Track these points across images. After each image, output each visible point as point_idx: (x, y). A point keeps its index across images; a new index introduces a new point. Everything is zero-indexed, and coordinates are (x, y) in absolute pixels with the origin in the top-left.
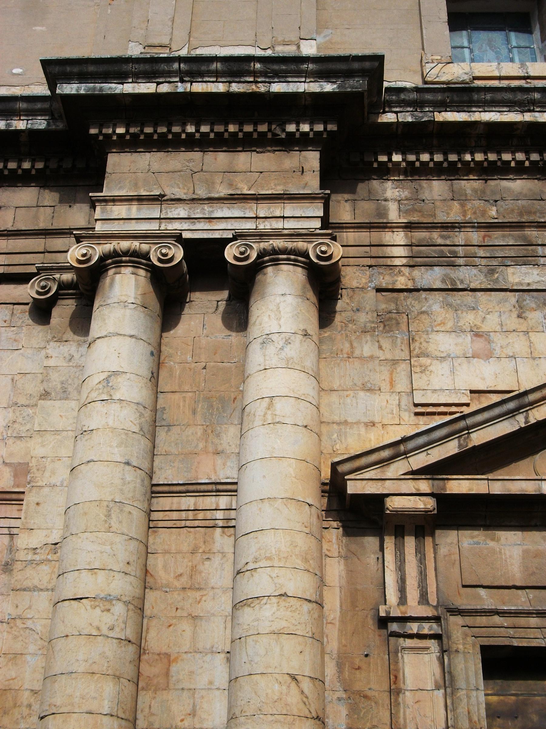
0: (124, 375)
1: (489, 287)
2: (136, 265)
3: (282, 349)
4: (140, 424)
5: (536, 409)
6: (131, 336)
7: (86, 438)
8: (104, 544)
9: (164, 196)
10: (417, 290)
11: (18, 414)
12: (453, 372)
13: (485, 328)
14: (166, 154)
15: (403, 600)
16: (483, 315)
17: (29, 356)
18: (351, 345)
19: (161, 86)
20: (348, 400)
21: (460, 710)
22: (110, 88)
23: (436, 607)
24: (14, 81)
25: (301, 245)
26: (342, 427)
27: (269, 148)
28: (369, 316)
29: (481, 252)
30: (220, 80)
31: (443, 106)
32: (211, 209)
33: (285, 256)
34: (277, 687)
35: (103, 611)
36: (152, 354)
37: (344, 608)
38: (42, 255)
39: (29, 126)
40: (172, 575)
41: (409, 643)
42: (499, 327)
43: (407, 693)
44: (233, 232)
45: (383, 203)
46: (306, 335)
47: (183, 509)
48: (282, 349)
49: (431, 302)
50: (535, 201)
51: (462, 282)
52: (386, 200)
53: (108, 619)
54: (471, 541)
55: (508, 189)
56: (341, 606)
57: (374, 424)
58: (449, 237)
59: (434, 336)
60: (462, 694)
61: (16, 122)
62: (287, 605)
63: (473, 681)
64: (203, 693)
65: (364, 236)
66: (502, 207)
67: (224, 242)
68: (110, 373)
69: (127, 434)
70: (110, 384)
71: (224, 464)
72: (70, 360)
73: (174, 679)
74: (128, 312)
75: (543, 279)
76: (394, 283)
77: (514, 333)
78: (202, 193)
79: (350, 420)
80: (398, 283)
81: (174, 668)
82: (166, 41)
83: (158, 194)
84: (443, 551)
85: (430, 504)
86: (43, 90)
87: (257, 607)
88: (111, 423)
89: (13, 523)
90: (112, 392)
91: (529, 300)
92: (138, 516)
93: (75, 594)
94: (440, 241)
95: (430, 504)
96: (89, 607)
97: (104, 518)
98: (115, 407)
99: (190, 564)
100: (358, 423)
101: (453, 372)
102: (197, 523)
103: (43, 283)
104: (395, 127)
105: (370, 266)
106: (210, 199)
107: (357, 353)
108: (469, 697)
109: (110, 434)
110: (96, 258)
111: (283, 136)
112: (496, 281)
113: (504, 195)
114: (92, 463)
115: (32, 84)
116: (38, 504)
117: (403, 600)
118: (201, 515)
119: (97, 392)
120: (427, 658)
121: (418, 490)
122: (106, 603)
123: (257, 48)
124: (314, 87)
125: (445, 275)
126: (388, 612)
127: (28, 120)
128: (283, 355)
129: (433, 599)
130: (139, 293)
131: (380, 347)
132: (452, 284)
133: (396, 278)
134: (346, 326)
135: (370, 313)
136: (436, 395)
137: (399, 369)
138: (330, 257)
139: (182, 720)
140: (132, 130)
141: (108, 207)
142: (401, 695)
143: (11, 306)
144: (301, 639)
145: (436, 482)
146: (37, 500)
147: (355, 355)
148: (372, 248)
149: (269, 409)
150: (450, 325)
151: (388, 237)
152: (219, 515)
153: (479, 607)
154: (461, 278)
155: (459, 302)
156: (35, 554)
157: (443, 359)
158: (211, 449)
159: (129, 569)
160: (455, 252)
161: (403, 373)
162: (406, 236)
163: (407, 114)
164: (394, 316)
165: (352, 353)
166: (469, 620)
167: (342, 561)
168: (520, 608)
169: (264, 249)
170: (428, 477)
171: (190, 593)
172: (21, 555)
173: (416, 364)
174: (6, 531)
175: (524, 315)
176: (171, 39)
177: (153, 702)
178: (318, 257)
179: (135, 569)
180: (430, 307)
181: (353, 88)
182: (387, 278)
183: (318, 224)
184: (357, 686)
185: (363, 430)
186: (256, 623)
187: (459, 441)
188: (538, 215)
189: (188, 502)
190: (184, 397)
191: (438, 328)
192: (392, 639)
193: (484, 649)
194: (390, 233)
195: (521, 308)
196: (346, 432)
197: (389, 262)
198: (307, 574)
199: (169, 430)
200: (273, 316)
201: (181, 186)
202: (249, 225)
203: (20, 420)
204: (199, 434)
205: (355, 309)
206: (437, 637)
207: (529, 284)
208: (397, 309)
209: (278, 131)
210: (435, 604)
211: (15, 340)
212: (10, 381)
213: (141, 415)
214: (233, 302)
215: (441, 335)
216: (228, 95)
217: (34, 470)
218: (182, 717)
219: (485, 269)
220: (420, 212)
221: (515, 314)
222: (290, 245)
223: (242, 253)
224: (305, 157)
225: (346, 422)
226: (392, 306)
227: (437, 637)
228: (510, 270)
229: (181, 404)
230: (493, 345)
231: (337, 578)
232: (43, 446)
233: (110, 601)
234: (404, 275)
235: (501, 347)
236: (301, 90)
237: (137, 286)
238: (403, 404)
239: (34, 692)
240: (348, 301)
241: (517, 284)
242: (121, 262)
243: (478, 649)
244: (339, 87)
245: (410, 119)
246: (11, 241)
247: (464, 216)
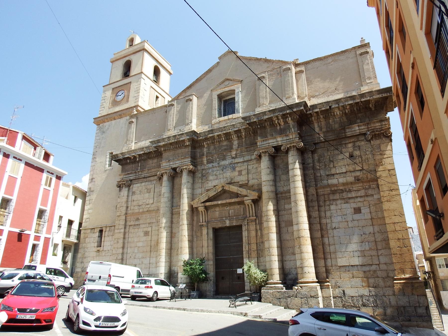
36: (170, 188)
55: (223, 145)
60: (209, 235)
74: (166, 182)
94: (211, 158)
213: (168, 198)
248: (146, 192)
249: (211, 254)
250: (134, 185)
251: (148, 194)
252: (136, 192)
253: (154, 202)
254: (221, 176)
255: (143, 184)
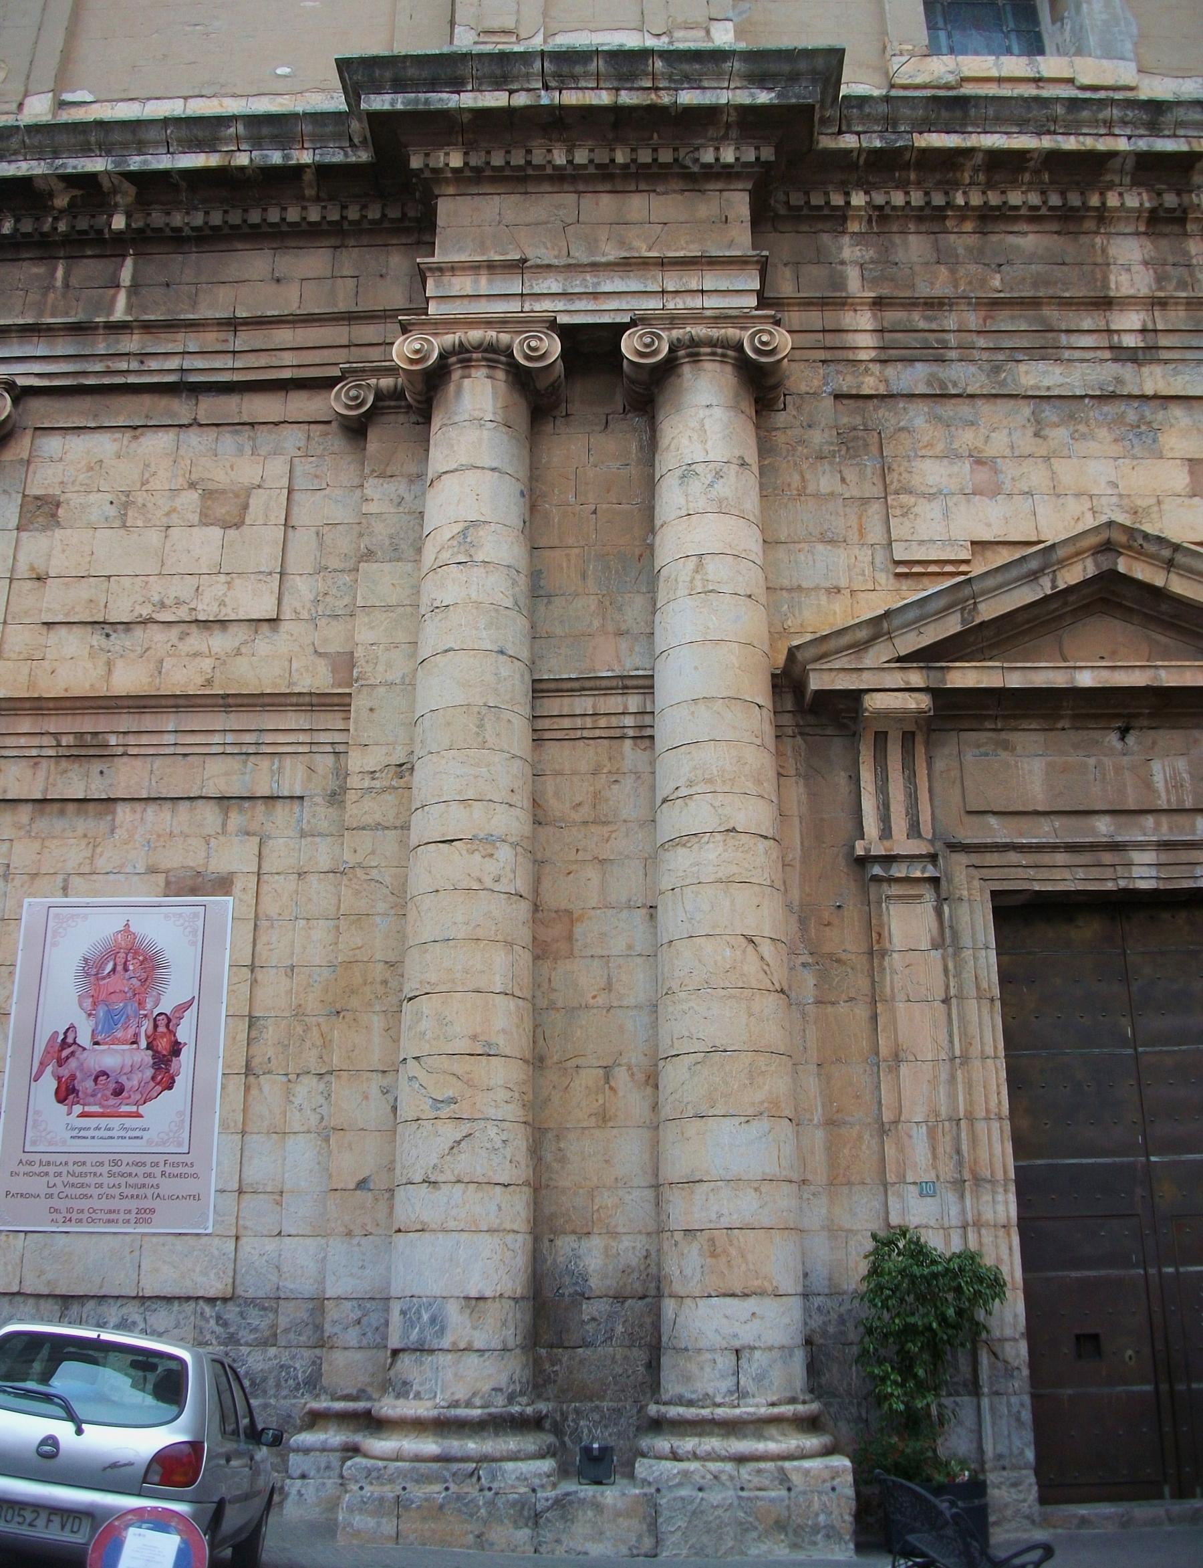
0: (487, 527)
1: (994, 392)
2: (492, 365)
3: (710, 485)
4: (513, 596)
5: (1066, 569)
6: (493, 470)
7: (440, 617)
8: (478, 765)
9: (525, 261)
10: (892, 396)
11: (330, 582)
12: (946, 515)
13: (990, 452)
14: (523, 197)
15: (886, 832)
16: (987, 433)
17: (339, 498)
18: (803, 477)
19: (515, 96)
20: (802, 557)
21: (965, 975)
22: (441, 100)
23: (932, 842)
24: (279, 86)
25: (732, 333)
26: (795, 595)
27: (677, 188)
28: (826, 435)
29: (982, 342)
30: (602, 85)
31: (927, 126)
32: (595, 280)
33: (708, 350)
34: (728, 952)
35: (484, 857)
36: (522, 494)
37: (806, 844)
38: (346, 350)
39: (317, 158)
40: (568, 805)
41: (895, 890)
42: (1008, 450)
43: (895, 955)
44: (631, 314)
45: (839, 267)
46: (743, 464)
47: (578, 712)
48: (710, 485)
49: (912, 414)
50: (1055, 267)
51: (955, 385)
52: (842, 263)
53: (491, 867)
54: (976, 751)
56: (802, 843)
57: (838, 590)
58: (936, 319)
59: (919, 465)
60: (967, 954)
61: (297, 152)
62: (737, 843)
63: (981, 937)
64: (621, 961)
65: (814, 318)
66: (1008, 274)
67: (618, 330)
68: (466, 524)
69: (497, 610)
70: (469, 540)
71: (631, 650)
72: (399, 504)
73: (579, 944)
75: (1068, 380)
76: (859, 387)
77: (1030, 459)
78: (581, 255)
79: (804, 585)
80: (865, 386)
81: (578, 930)
82: (509, 24)
83: (518, 257)
84: (939, 765)
85: (923, 702)
86: (337, 102)
87: (696, 847)
88: (474, 596)
89: (338, 737)
90: (472, 551)
91: (1049, 413)
92: (519, 727)
93: (443, 835)
94: (922, 325)
95: (923, 702)
96: (464, 852)
97: (475, 729)
98: (479, 572)
99: (592, 788)
100: (817, 588)
101: (946, 515)
102: (597, 733)
103: (353, 393)
104: (855, 154)
105: (823, 362)
106: (595, 266)
107: (811, 488)
108: (975, 958)
109: (474, 611)
110: (435, 355)
111: (696, 169)
112: (1003, 383)
113: (1011, 257)
114: (452, 653)
115: (307, 91)
116: (371, 710)
117: (886, 832)
118: (603, 722)
119: (450, 552)
120: (919, 908)
121: (908, 683)
122: (488, 846)
123: (646, 34)
124: (743, 97)
125: (931, 375)
126: (868, 850)
127: (314, 149)
128: (713, 494)
129: (926, 829)
130: (499, 405)
131: (843, 480)
132: (941, 388)
133: (861, 378)
134: (794, 449)
135: (826, 430)
136: (924, 549)
137: (870, 512)
138: (772, 352)
139: (594, 997)
140: (474, 162)
141: (445, 279)
142: (887, 958)
143: (306, 427)
144: (756, 888)
145: (932, 674)
146: (369, 705)
147: (808, 491)
148: (827, 335)
149: (697, 572)
150: (940, 447)
151: (848, 319)
152: (629, 721)
153: (989, 840)
154: (955, 378)
155: (951, 413)
156: (373, 779)
157: (931, 497)
158: (610, 628)
159: (515, 799)
160: (945, 341)
161: (876, 517)
162: (874, 316)
163: (874, 135)
164: (860, 434)
165: (804, 488)
166: (975, 859)
167: (801, 782)
168: (1044, 840)
169: (678, 339)
170: (922, 665)
171: (593, 829)
172: (353, 781)
173: (895, 503)
174: (329, 749)
175: (1042, 433)
176: (517, 21)
177: (553, 974)
178: (757, 351)
179: (522, 800)
180: (911, 420)
181: (798, 97)
182: (849, 378)
183: (752, 301)
184: (826, 949)
185: (824, 598)
186: (695, 869)
187: (962, 614)
188: (1059, 285)
189: (584, 704)
190: (568, 555)
191: (923, 452)
192: (873, 888)
193: (994, 894)
194: (851, 313)
195: (1038, 422)
196: (800, 603)
197: (850, 355)
198: (761, 802)
199: (549, 602)
200: (695, 437)
201: (549, 245)
202: (653, 303)
203: (334, 591)
204: (593, 607)
205: (805, 424)
206: (935, 881)
207: (1048, 388)
208: (864, 424)
209: (688, 162)
210: (930, 837)
211: (317, 476)
212: (314, 536)
213: (514, 583)
214: (630, 415)
215: (928, 461)
216: (616, 110)
217: (362, 662)
218: (595, 993)
219: (987, 366)
220: (892, 280)
221: (1030, 432)
222: (715, 333)
223: (647, 346)
224: (727, 200)
225: (799, 587)
226: (858, 420)
227: (935, 881)
228: (1022, 368)
229: (565, 565)
230: (1002, 476)
231: (795, 803)
232: (372, 628)
233: (493, 843)
234: (872, 375)
235: (1013, 479)
236: (724, 101)
237: (495, 393)
238: (878, 560)
239: (390, 965)
240: (795, 413)
241: (1032, 388)
242: (470, 360)
243: (988, 896)
244: (778, 96)
245: (878, 144)
246: (299, 331)
247: (956, 287)
248: (195, 518)
249: (996, 1125)
250: (52, 445)
251: (215, 532)
252: (75, 499)
253: (287, 614)
254: (1036, 476)
255: (157, 443)
